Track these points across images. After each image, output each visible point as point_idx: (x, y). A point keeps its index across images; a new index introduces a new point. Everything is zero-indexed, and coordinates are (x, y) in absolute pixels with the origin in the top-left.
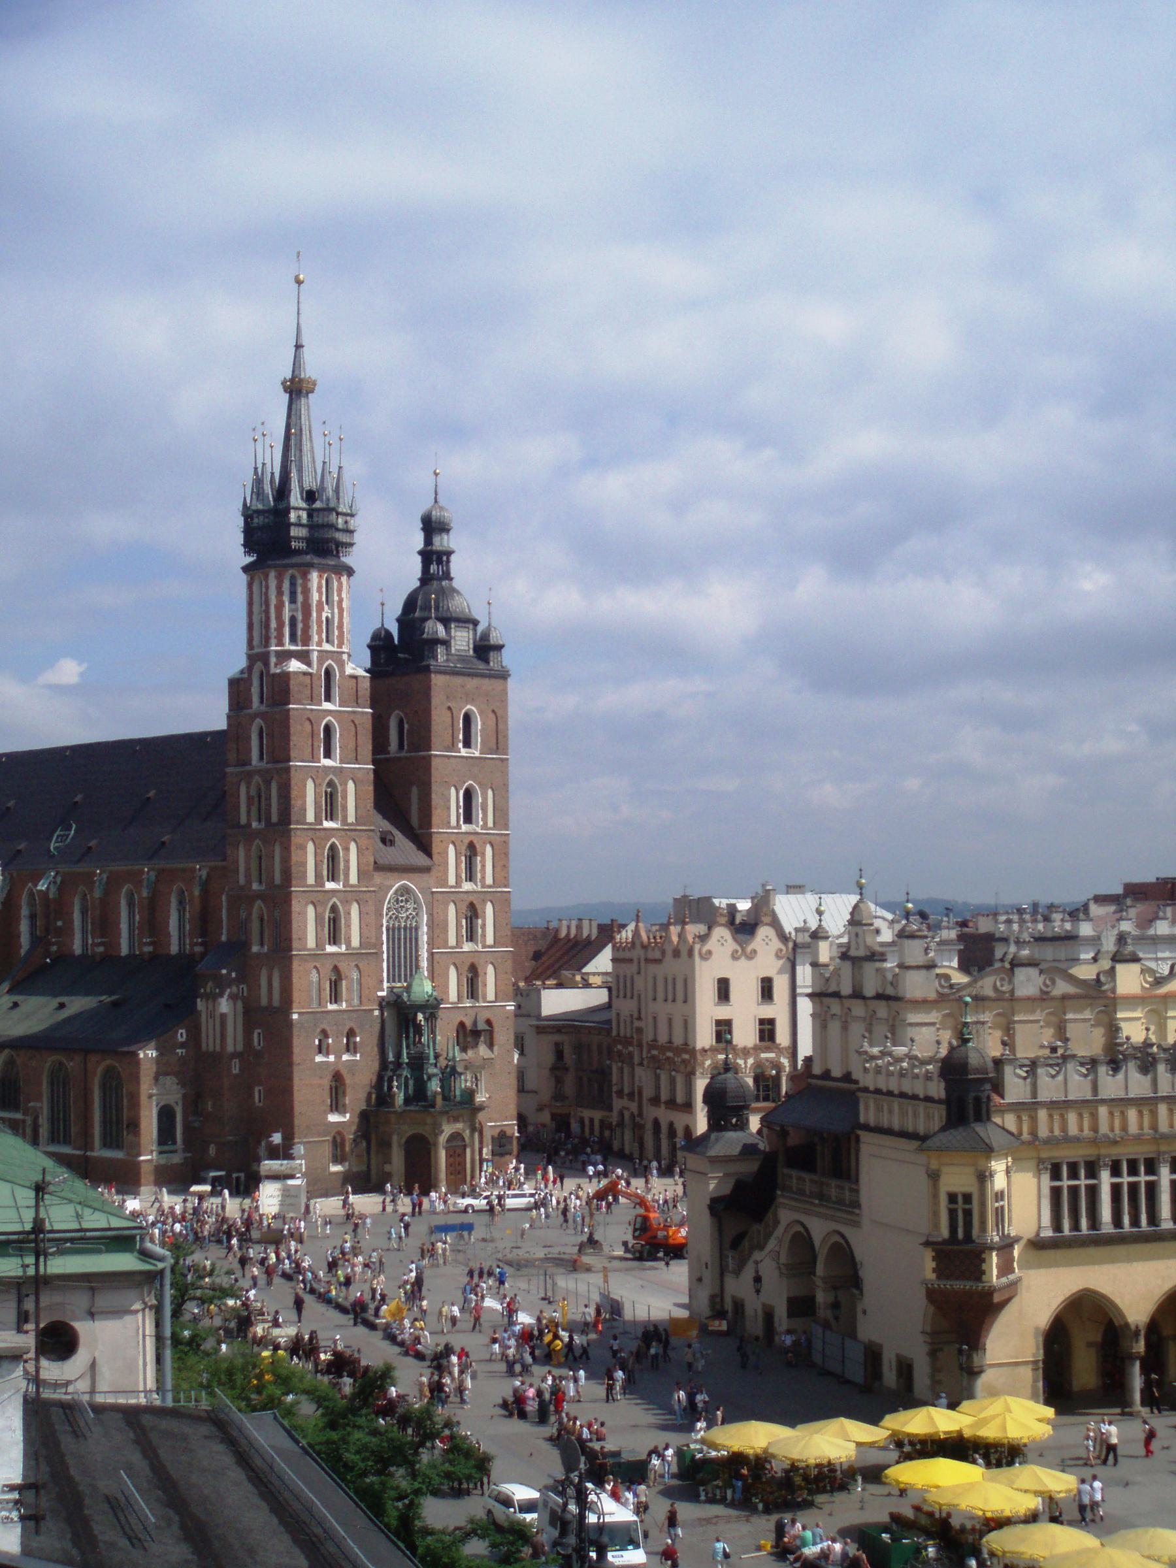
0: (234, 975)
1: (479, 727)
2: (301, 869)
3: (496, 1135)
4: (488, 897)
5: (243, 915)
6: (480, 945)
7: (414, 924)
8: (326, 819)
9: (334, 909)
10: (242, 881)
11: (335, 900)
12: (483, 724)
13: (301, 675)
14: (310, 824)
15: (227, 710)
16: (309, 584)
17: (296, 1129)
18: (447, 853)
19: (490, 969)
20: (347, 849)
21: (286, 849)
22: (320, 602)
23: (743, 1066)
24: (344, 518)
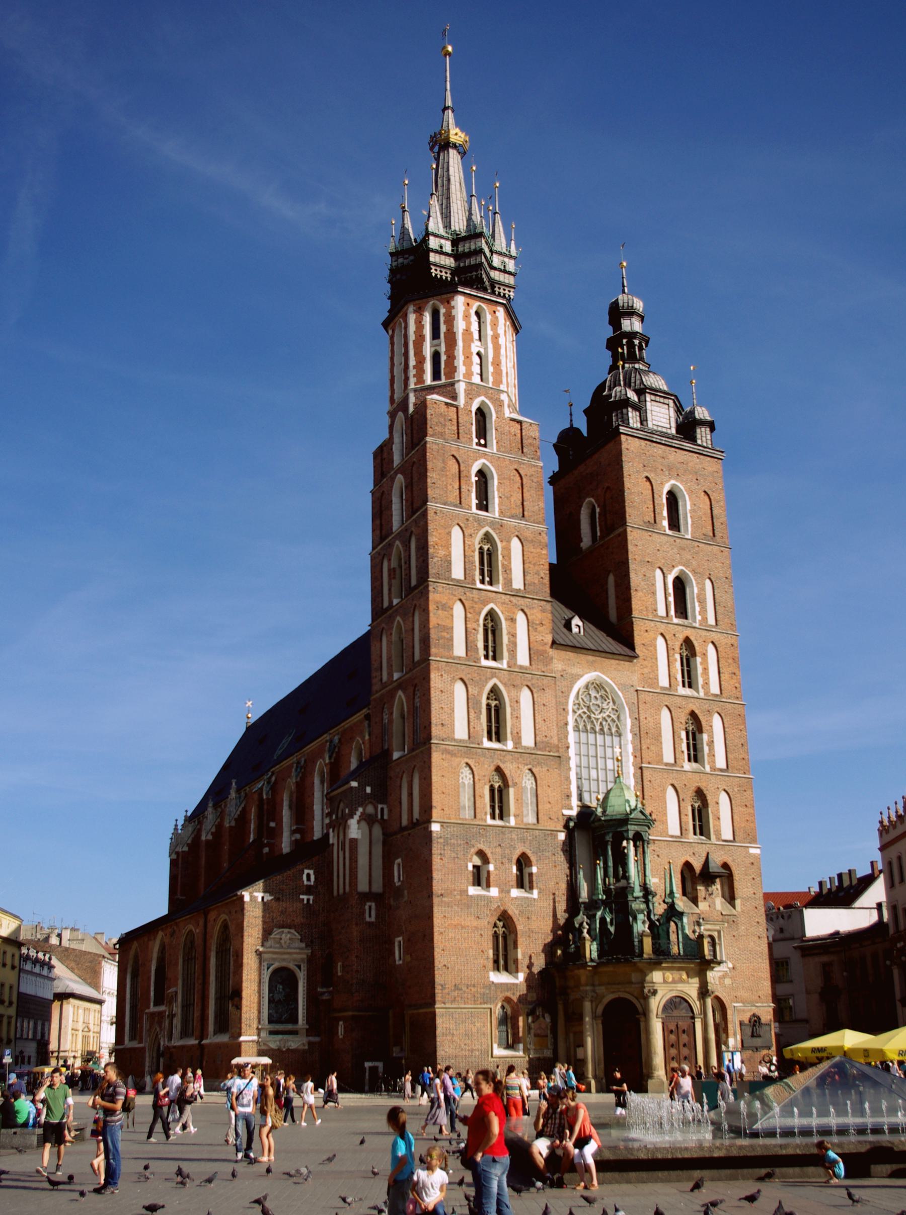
0: (368, 790)
1: (689, 507)
2: (445, 634)
3: (747, 1021)
4: (715, 707)
5: (385, 717)
6: (708, 769)
7: (614, 730)
8: (482, 582)
9: (495, 692)
10: (385, 678)
11: (494, 681)
13: (443, 408)
14: (458, 581)
15: (371, 487)
16: (454, 312)
17: (438, 990)
18: (655, 647)
19: (723, 798)
20: (513, 620)
21: (426, 611)
22: (467, 331)
24: (500, 257)
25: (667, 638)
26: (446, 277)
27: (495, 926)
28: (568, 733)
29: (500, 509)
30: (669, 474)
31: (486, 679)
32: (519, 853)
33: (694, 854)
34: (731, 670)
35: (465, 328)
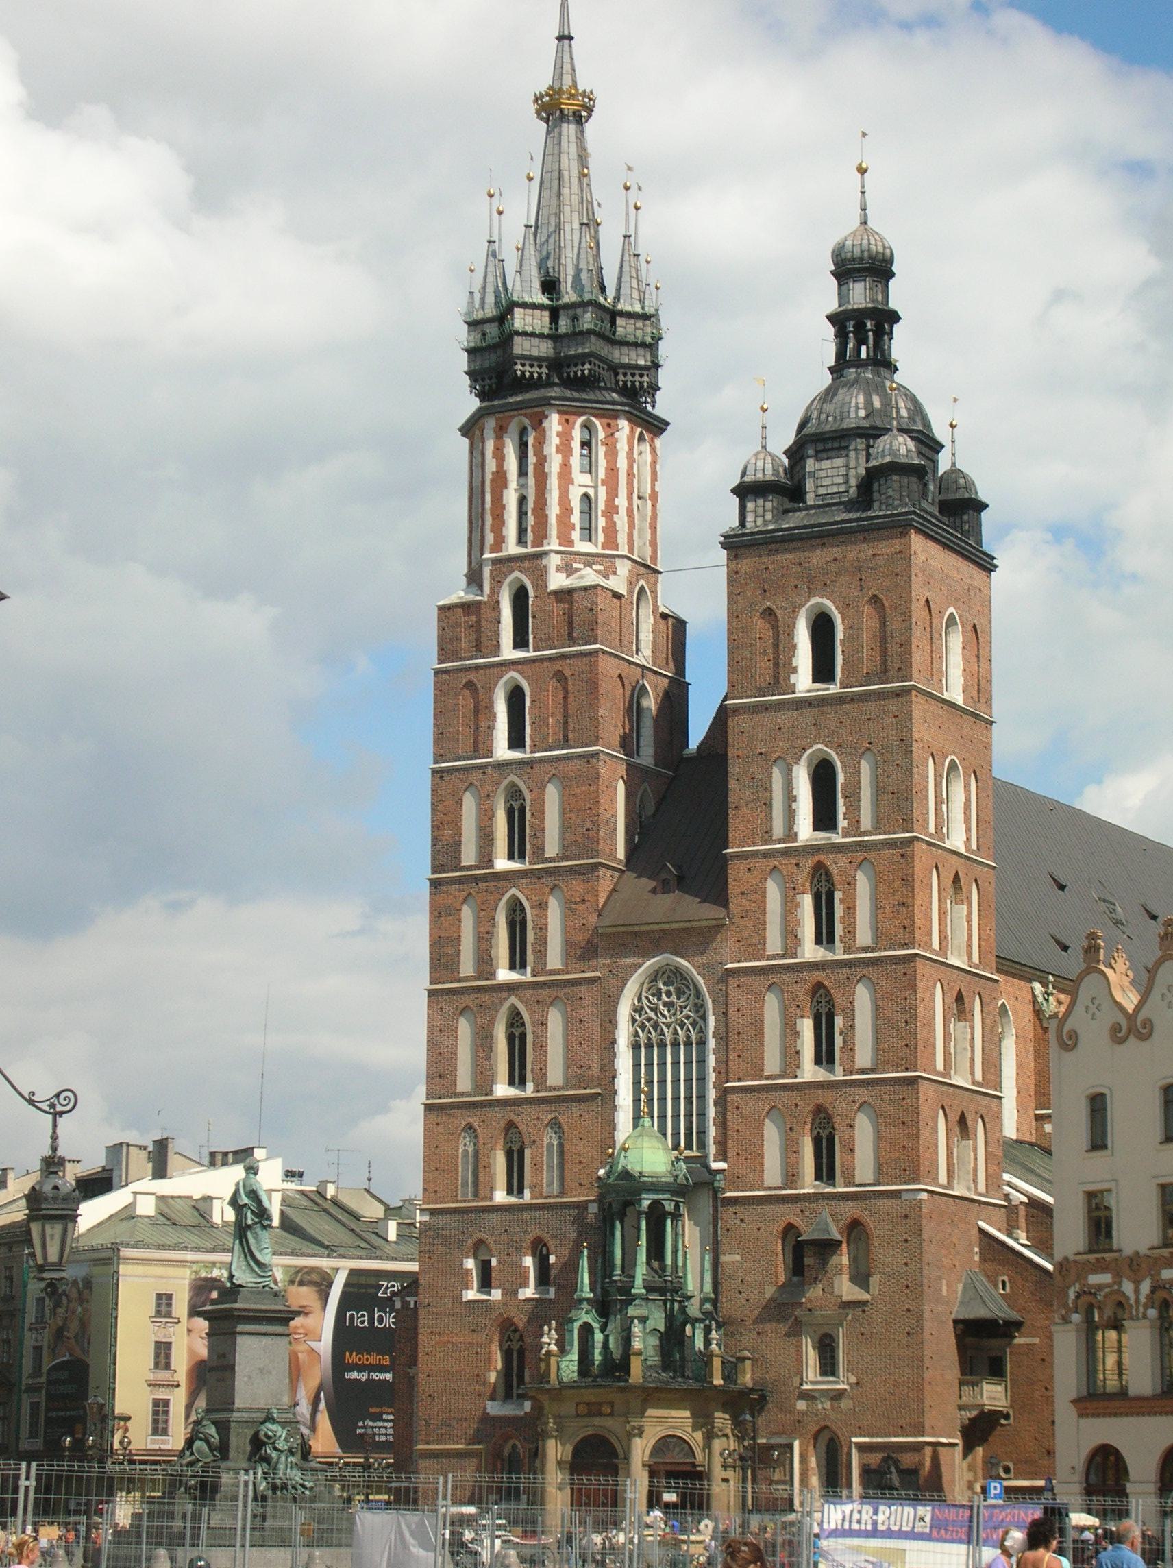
2: (450, 950)
11: (513, 1000)
12: (849, 627)
13: (460, 611)
18: (764, 892)
20: (542, 906)
23: (1132, 1301)
25: (785, 873)
26: (490, 386)
27: (509, 1339)
28: (614, 1055)
29: (532, 741)
30: (809, 588)
31: (501, 1001)
32: (532, 1239)
33: (802, 1211)
34: (898, 897)
35: (494, 469)
